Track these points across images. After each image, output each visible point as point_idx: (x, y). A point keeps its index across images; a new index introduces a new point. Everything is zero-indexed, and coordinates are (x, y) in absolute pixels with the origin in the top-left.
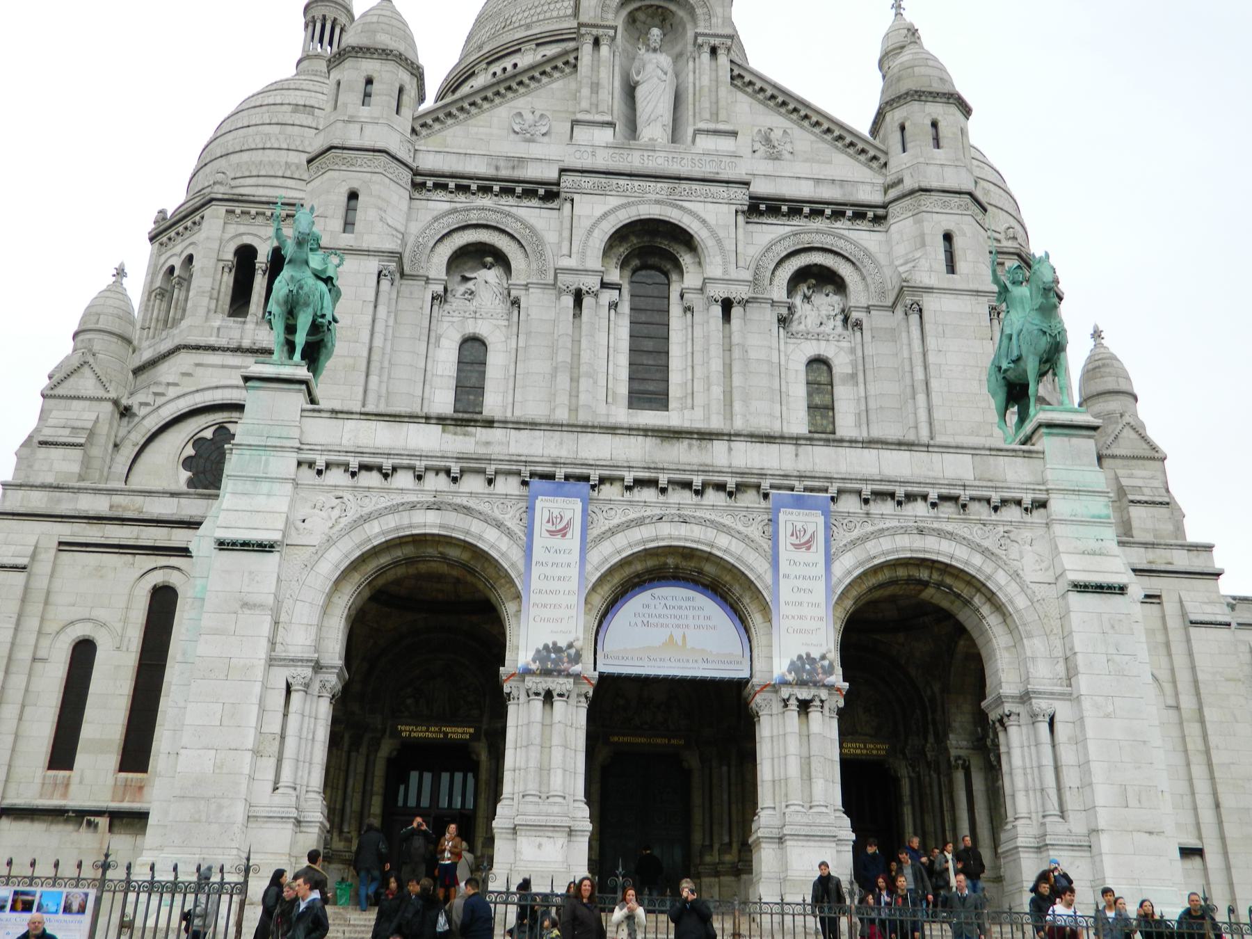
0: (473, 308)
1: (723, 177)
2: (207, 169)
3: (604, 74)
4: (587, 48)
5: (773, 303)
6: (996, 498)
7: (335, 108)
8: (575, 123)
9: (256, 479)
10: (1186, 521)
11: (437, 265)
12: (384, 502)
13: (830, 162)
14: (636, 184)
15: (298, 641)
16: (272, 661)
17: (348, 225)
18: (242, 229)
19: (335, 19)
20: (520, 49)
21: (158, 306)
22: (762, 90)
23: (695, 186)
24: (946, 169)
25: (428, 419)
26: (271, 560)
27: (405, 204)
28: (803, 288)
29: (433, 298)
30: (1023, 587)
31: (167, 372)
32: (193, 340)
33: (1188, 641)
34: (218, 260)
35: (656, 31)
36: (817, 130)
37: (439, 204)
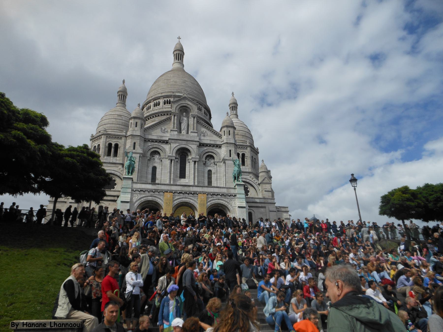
2: (101, 127)
3: (175, 121)
6: (229, 195)
7: (131, 127)
8: (171, 130)
9: (125, 192)
10: (274, 194)
12: (144, 196)
13: (213, 137)
14: (181, 141)
17: (134, 149)
18: (109, 140)
23: (191, 142)
24: (231, 139)
25: (150, 184)
26: (128, 204)
27: (143, 144)
30: (232, 207)
33: (269, 214)
34: (105, 146)
35: (184, 113)
37: (149, 144)
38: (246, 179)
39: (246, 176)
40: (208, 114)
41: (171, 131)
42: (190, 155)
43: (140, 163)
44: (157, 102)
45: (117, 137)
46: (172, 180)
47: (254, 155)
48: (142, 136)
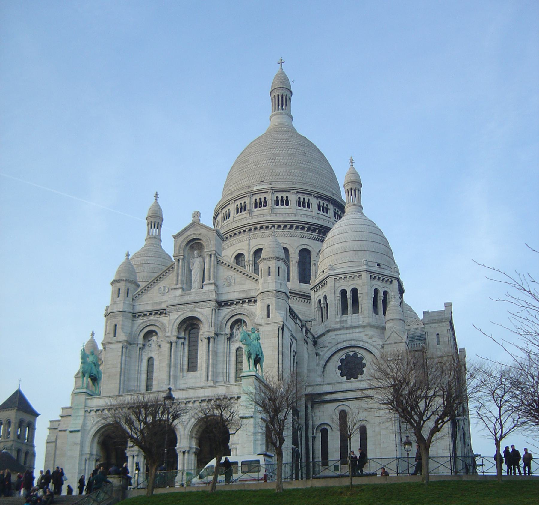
0: (150, 349)
3: (180, 271)
9: (77, 416)
11: (140, 340)
13: (245, 284)
15: (87, 450)
16: (81, 454)
19: (155, 222)
20: (229, 204)
22: (226, 264)
23: (201, 304)
24: (270, 284)
26: (79, 434)
27: (130, 325)
28: (236, 326)
29: (140, 349)
36: (241, 274)
37: (140, 321)
39: (357, 335)
42: (202, 328)
43: (124, 357)
44: (226, 211)
46: (172, 377)
47: (385, 285)
48: (127, 310)
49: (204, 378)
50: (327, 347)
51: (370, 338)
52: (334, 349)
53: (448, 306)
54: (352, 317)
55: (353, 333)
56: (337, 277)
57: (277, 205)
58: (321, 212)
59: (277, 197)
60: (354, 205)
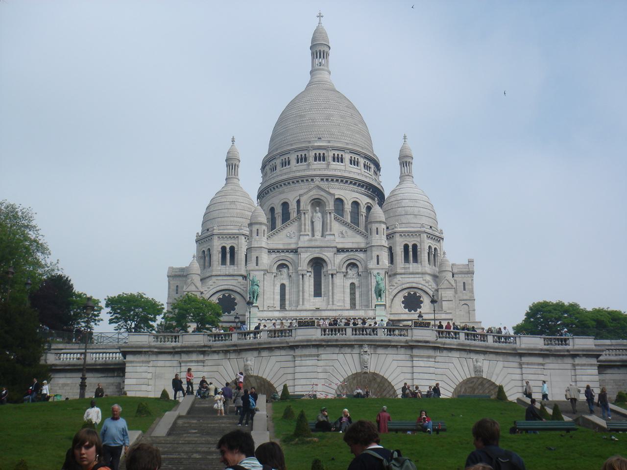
1: (332, 246)
2: (209, 222)
3: (307, 222)
4: (303, 215)
5: (342, 272)
17: (257, 265)
18: (222, 242)
21: (202, 261)
23: (326, 249)
25: (277, 311)
27: (267, 258)
28: (350, 267)
31: (210, 282)
32: (214, 273)
35: (317, 208)
37: (274, 255)
38: (417, 283)
39: (417, 279)
40: (372, 166)
41: (301, 237)
44: (285, 159)
45: (232, 237)
47: (435, 243)
49: (331, 303)
50: (394, 286)
51: (426, 282)
52: (400, 288)
53: (471, 261)
54: (413, 265)
55: (414, 278)
56: (403, 234)
57: (334, 161)
58: (366, 171)
59: (334, 154)
60: (408, 175)
